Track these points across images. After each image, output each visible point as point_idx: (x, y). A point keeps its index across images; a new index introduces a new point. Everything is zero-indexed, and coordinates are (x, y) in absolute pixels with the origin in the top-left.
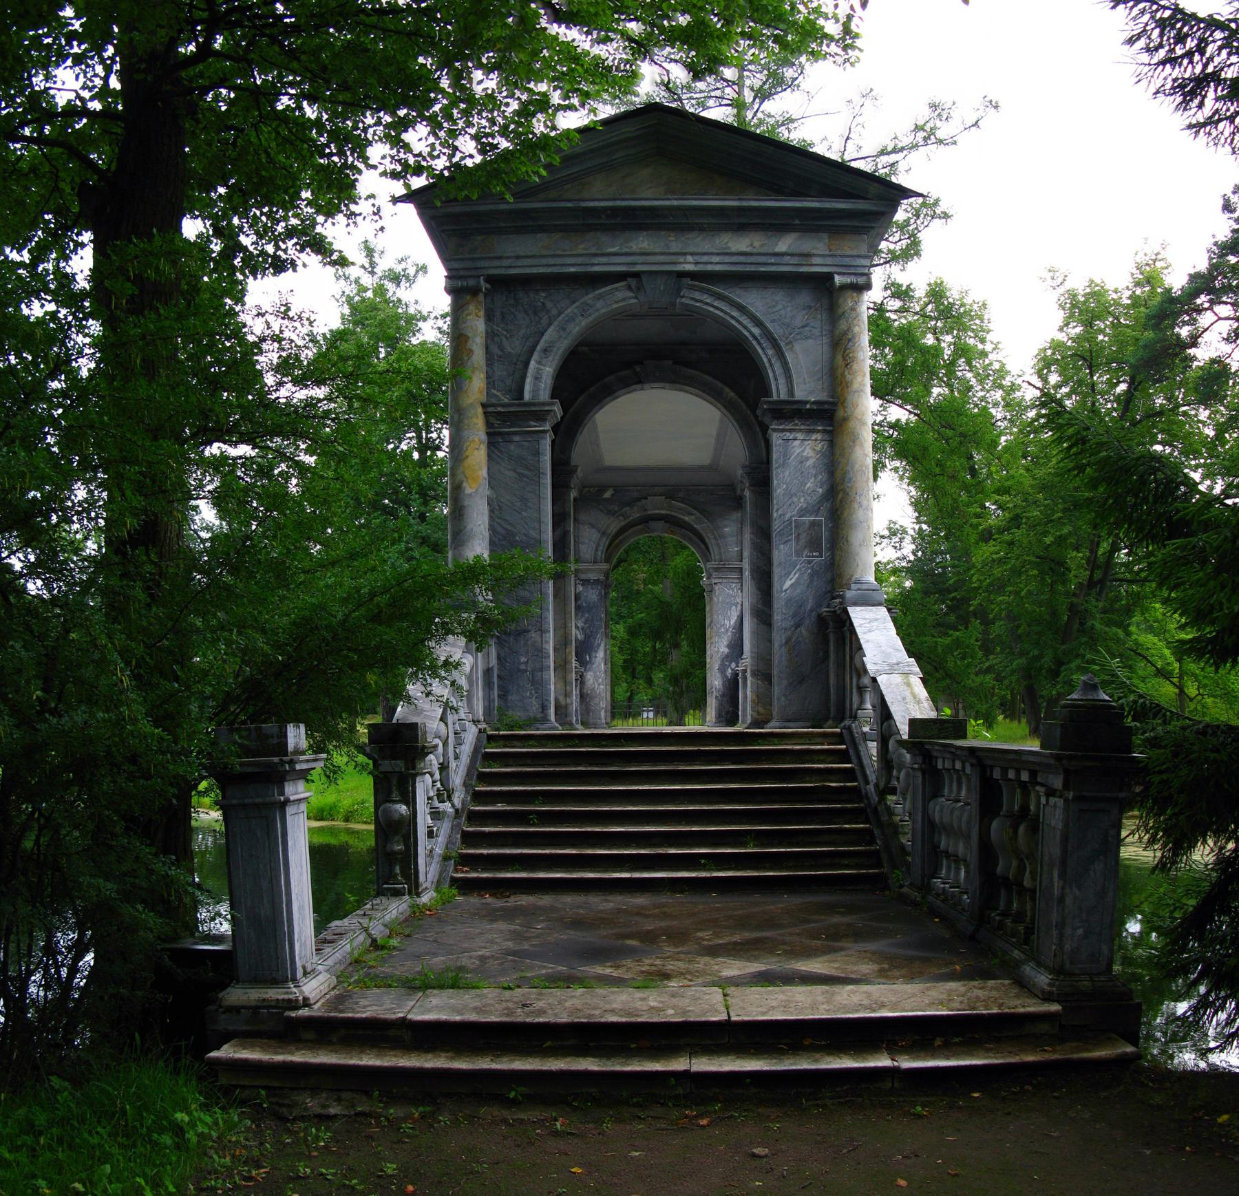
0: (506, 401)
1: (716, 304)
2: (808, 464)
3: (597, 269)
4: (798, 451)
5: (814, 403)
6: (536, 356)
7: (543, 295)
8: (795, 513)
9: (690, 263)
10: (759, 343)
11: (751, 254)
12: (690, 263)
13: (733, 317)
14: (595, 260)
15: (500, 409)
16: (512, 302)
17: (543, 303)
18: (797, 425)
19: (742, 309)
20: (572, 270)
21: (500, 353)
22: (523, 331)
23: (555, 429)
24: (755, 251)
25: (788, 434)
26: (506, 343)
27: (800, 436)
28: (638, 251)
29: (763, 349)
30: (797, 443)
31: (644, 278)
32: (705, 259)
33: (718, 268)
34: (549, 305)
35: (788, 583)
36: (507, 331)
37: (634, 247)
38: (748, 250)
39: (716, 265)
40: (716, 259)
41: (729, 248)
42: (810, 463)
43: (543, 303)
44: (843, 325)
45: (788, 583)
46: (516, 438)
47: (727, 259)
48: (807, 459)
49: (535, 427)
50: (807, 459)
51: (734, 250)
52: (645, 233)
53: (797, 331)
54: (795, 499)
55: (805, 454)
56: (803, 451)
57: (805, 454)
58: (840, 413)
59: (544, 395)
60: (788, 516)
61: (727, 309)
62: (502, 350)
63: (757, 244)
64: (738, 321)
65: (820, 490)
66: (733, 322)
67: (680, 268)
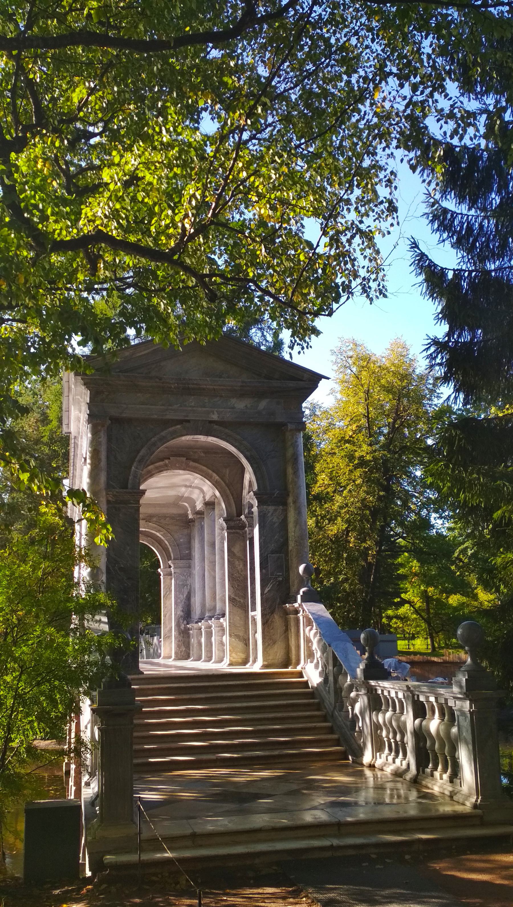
7: (139, 429)
35: (266, 591)
42: (276, 525)
45: (266, 591)
48: (275, 523)
50: (275, 523)
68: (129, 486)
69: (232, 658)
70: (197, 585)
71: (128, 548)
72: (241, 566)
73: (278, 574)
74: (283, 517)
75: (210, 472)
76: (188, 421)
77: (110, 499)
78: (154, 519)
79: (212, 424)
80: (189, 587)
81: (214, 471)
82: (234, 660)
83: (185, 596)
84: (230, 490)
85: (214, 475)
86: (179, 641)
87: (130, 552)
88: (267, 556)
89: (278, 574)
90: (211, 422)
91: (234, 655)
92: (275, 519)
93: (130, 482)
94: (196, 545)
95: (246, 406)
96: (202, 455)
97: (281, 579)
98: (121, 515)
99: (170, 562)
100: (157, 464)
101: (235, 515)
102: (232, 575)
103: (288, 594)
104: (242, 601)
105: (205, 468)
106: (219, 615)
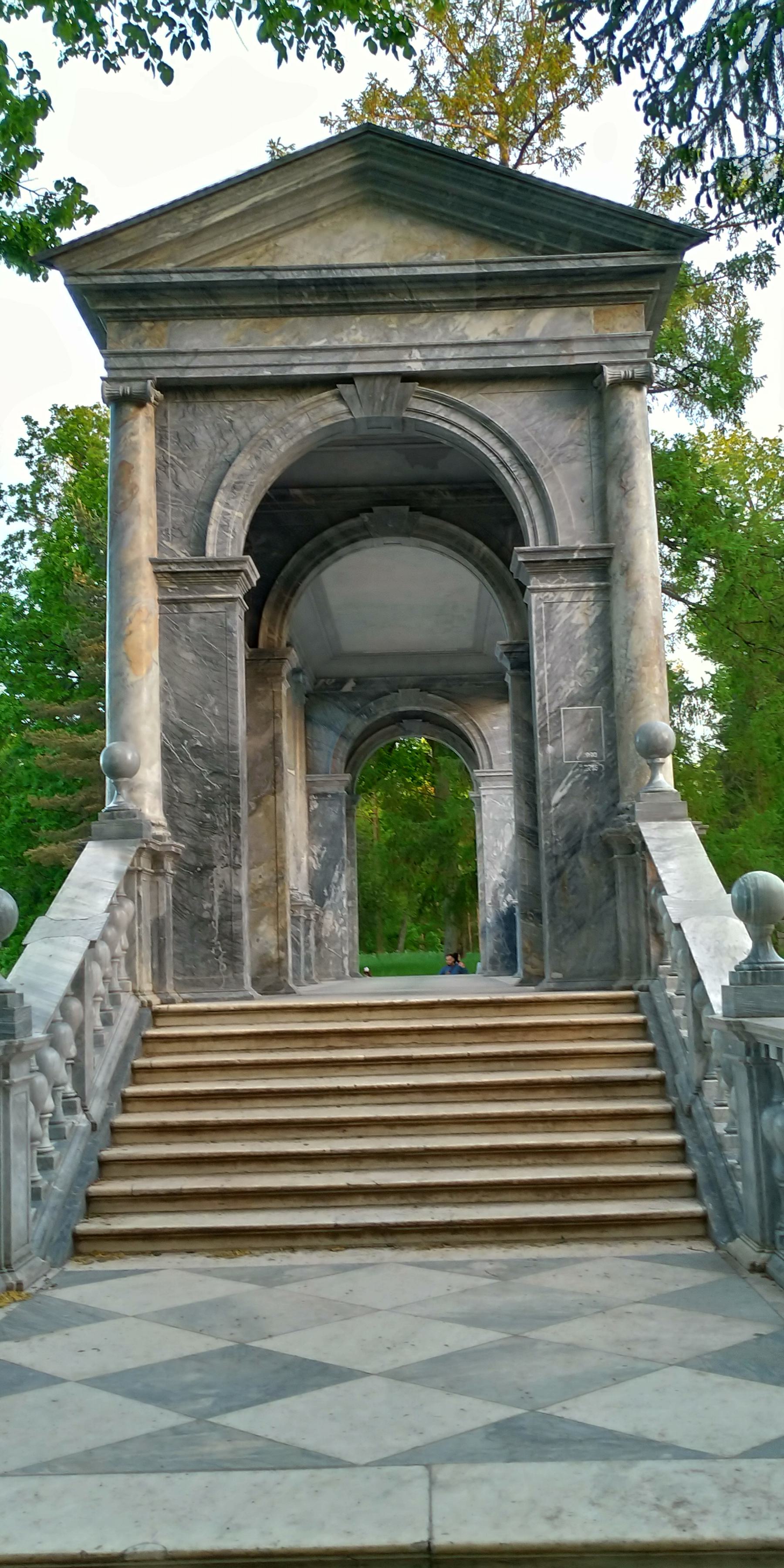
0: (183, 556)
2: (578, 635)
4: (565, 616)
5: (583, 550)
6: (221, 496)
7: (231, 408)
8: (564, 701)
9: (417, 360)
10: (509, 471)
11: (495, 344)
12: (417, 360)
13: (474, 437)
14: (295, 360)
15: (174, 568)
17: (231, 421)
18: (562, 582)
19: (486, 423)
20: (267, 372)
21: (175, 490)
22: (204, 461)
23: (249, 596)
24: (499, 339)
25: (551, 595)
26: (182, 477)
27: (567, 596)
28: (350, 344)
29: (514, 480)
30: (563, 606)
32: (436, 353)
33: (453, 366)
34: (238, 423)
35: (557, 796)
36: (183, 459)
37: (345, 340)
38: (491, 338)
40: (450, 353)
42: (582, 631)
43: (231, 421)
45: (557, 796)
46: (198, 608)
47: (464, 353)
48: (577, 627)
49: (221, 592)
51: (472, 339)
52: (358, 319)
53: (558, 451)
54: (563, 683)
56: (571, 617)
57: (574, 621)
59: (234, 548)
60: (555, 705)
63: (502, 330)
64: (481, 441)
66: (475, 443)
67: (403, 368)
71: (212, 700)
73: (588, 754)
74: (597, 614)
76: (349, 379)
79: (410, 384)
87: (216, 711)
88: (558, 711)
89: (588, 754)
95: (495, 331)
97: (593, 767)
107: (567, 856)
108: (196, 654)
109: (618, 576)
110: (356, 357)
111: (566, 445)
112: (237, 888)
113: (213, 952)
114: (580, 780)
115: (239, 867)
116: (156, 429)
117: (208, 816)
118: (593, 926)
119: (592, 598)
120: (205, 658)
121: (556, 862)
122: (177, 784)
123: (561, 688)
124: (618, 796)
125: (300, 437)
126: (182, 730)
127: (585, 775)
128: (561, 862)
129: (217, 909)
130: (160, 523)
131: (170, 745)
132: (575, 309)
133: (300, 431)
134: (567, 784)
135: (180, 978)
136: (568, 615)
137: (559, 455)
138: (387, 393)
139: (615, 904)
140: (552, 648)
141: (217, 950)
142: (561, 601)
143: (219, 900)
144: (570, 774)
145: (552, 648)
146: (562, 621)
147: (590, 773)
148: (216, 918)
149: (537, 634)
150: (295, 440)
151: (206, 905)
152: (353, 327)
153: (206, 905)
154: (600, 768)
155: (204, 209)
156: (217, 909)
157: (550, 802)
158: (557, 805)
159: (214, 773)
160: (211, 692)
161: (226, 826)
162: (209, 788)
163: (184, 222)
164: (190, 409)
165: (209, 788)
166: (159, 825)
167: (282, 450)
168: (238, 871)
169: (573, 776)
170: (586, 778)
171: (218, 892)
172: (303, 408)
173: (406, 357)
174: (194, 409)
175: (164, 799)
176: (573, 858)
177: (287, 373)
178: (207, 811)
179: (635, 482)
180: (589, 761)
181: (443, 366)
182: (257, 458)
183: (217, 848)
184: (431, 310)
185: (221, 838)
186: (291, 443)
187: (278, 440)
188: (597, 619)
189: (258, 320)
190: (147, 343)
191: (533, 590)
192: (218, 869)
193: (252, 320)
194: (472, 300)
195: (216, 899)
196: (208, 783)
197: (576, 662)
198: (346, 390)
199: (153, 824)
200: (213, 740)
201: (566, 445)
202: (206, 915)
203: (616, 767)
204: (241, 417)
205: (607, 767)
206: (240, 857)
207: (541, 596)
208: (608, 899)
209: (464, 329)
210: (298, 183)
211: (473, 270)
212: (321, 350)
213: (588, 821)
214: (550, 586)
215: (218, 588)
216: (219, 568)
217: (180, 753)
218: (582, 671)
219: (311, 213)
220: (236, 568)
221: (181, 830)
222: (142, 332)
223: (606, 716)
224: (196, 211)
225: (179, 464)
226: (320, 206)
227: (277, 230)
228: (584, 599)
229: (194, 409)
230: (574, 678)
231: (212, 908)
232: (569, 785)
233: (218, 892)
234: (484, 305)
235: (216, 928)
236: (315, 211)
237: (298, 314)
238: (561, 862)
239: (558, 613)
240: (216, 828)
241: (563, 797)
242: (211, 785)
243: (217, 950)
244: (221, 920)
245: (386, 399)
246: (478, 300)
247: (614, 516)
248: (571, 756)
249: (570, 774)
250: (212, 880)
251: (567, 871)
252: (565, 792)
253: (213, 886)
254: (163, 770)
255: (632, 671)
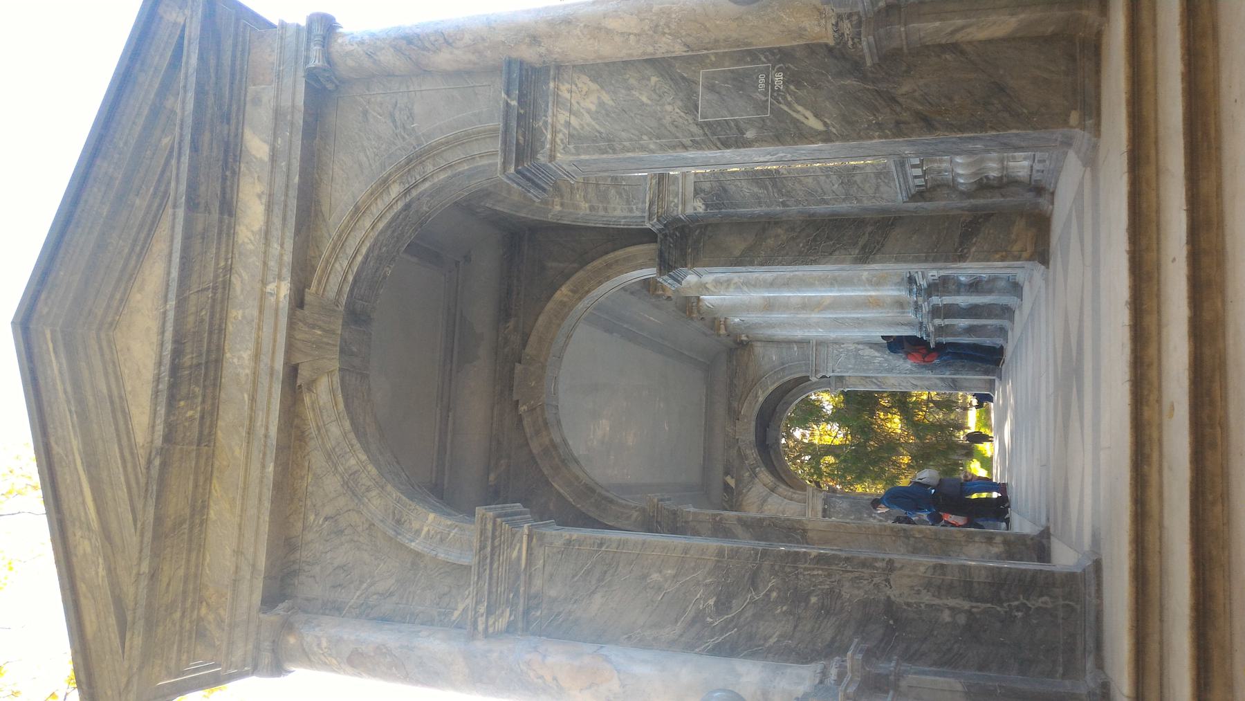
1: (350, 252)
2: (611, 103)
3: (273, 430)
5: (508, 93)
7: (312, 518)
8: (690, 118)
9: (278, 287)
10: (415, 186)
16: (317, 569)
17: (326, 519)
18: (546, 123)
20: (270, 468)
21: (394, 599)
29: (425, 180)
30: (574, 121)
31: (295, 361)
34: (329, 510)
35: (814, 123)
36: (361, 582)
37: (247, 371)
39: (283, 250)
41: (260, 230)
42: (606, 98)
43: (326, 519)
44: (388, 58)
45: (814, 123)
46: (538, 583)
47: (276, 232)
48: (601, 104)
52: (228, 355)
55: (593, 108)
56: (589, 111)
57: (593, 108)
58: (529, 54)
60: (694, 129)
61: (359, 235)
62: (391, 594)
64: (380, 218)
65: (654, 79)
66: (381, 226)
68: (465, 561)
69: (1025, 255)
70: (858, 334)
71: (655, 576)
72: (780, 231)
73: (762, 86)
74: (585, 78)
75: (550, 306)
76: (292, 371)
77: (502, 623)
78: (735, 404)
79: (308, 298)
80: (860, 347)
81: (549, 298)
82: (1030, 250)
83: (877, 354)
84: (593, 260)
85: (558, 295)
86: (963, 366)
87: (670, 572)
89: (762, 86)
90: (298, 301)
91: (1016, 248)
92: (590, 104)
93: (452, 558)
94: (781, 333)
95: (259, 197)
96: (511, 324)
97: (779, 78)
98: (553, 593)
99: (814, 379)
100: (529, 431)
101: (653, 246)
102: (800, 253)
103: (830, 50)
104: (869, 229)
105: (542, 320)
106: (910, 291)
107: (898, 109)
108: (593, 593)
109: (542, 50)
110: (265, 359)
111: (394, 121)
112: (922, 569)
113: (1020, 614)
114: (793, 94)
115: (891, 562)
116: (324, 614)
117: (813, 600)
118: (1001, 72)
119: (567, 86)
120: (600, 580)
121: (905, 123)
122: (766, 639)
123: (672, 123)
124: (820, 45)
125: (352, 436)
126: (693, 621)
127: (787, 90)
128: (906, 116)
129: (952, 602)
130: (429, 622)
131: (711, 643)
132: (248, 107)
133: (345, 435)
134: (798, 112)
135: (1061, 670)
136: (586, 114)
137: (404, 128)
138: (313, 326)
139: (970, 43)
140: (624, 135)
141: (1018, 609)
142: (568, 124)
143: (939, 597)
144: (785, 108)
145: (624, 135)
146: (593, 123)
147: (786, 83)
148: (966, 605)
149: (604, 152)
150: (355, 441)
151: (946, 616)
152: (235, 360)
153: (946, 616)
154: (778, 71)
155: (77, 524)
156: (952, 602)
157: (820, 133)
158: (825, 124)
159: (754, 583)
160: (645, 577)
161: (829, 575)
162: (774, 594)
163: (89, 550)
164: (307, 568)
165: (774, 594)
166: (824, 674)
167: (364, 457)
168: (897, 565)
169: (789, 104)
170: (792, 87)
171: (927, 598)
172: (319, 429)
173: (273, 299)
174: (308, 563)
175: (786, 661)
176: (901, 100)
177: (275, 443)
178: (807, 600)
179: (436, 32)
180: (769, 83)
181: (288, 258)
182: (368, 490)
183: (861, 593)
184: (229, 270)
185: (847, 584)
186: (358, 446)
187: (353, 462)
188: (594, 80)
189: (216, 474)
190: (221, 612)
191: (552, 158)
192: (893, 593)
193: (215, 481)
194: (221, 221)
195: (936, 601)
196: (767, 595)
197: (643, 104)
198: (305, 374)
199: (821, 682)
200: (708, 581)
201: (394, 121)
202: (962, 619)
203: (780, 49)
204: (324, 505)
205: (780, 61)
206: (876, 560)
207: (560, 147)
208: (963, 52)
209: (252, 231)
210: (70, 411)
211: (181, 213)
212: (253, 399)
213: (850, 82)
214: (549, 136)
215: (515, 554)
216: (489, 549)
217: (724, 629)
218: (655, 97)
219: (112, 402)
220: (490, 527)
221: (833, 640)
222: (211, 617)
223: (713, 65)
224: (79, 534)
225: (367, 589)
226: (105, 391)
227: (125, 441)
228: (568, 96)
229: (308, 563)
230: (663, 105)
231: (952, 609)
232: (800, 108)
233: (927, 598)
234: (228, 207)
235: (983, 606)
236: (111, 397)
237: (213, 425)
238: (906, 116)
239: (583, 128)
240: (832, 590)
241: (816, 116)
242: (771, 591)
243: (1018, 609)
244: (969, 597)
245: (320, 328)
246: (221, 213)
247: (473, 58)
248: (762, 106)
249: (785, 108)
250: (908, 604)
251: (920, 108)
252: (808, 114)
253: (918, 604)
254: (745, 657)
255: (657, 26)
